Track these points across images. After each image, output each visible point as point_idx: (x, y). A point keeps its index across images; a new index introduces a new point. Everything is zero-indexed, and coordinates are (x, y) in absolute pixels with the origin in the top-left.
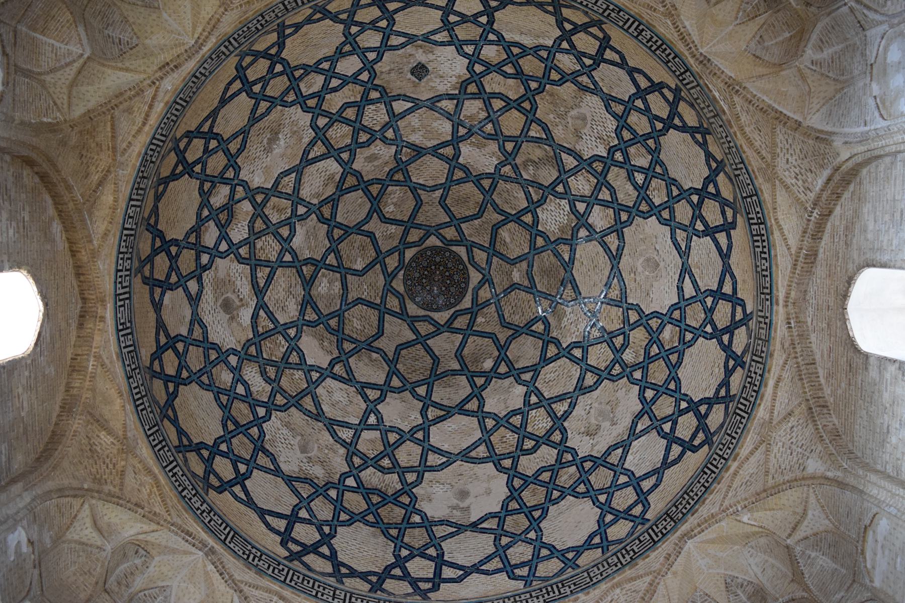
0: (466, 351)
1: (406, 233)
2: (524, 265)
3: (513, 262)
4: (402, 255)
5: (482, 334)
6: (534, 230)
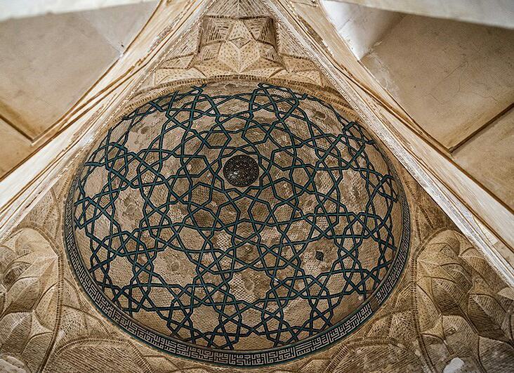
0: (203, 161)
1: (270, 179)
2: (215, 211)
3: (219, 208)
4: (264, 169)
5: (203, 172)
6: (225, 227)
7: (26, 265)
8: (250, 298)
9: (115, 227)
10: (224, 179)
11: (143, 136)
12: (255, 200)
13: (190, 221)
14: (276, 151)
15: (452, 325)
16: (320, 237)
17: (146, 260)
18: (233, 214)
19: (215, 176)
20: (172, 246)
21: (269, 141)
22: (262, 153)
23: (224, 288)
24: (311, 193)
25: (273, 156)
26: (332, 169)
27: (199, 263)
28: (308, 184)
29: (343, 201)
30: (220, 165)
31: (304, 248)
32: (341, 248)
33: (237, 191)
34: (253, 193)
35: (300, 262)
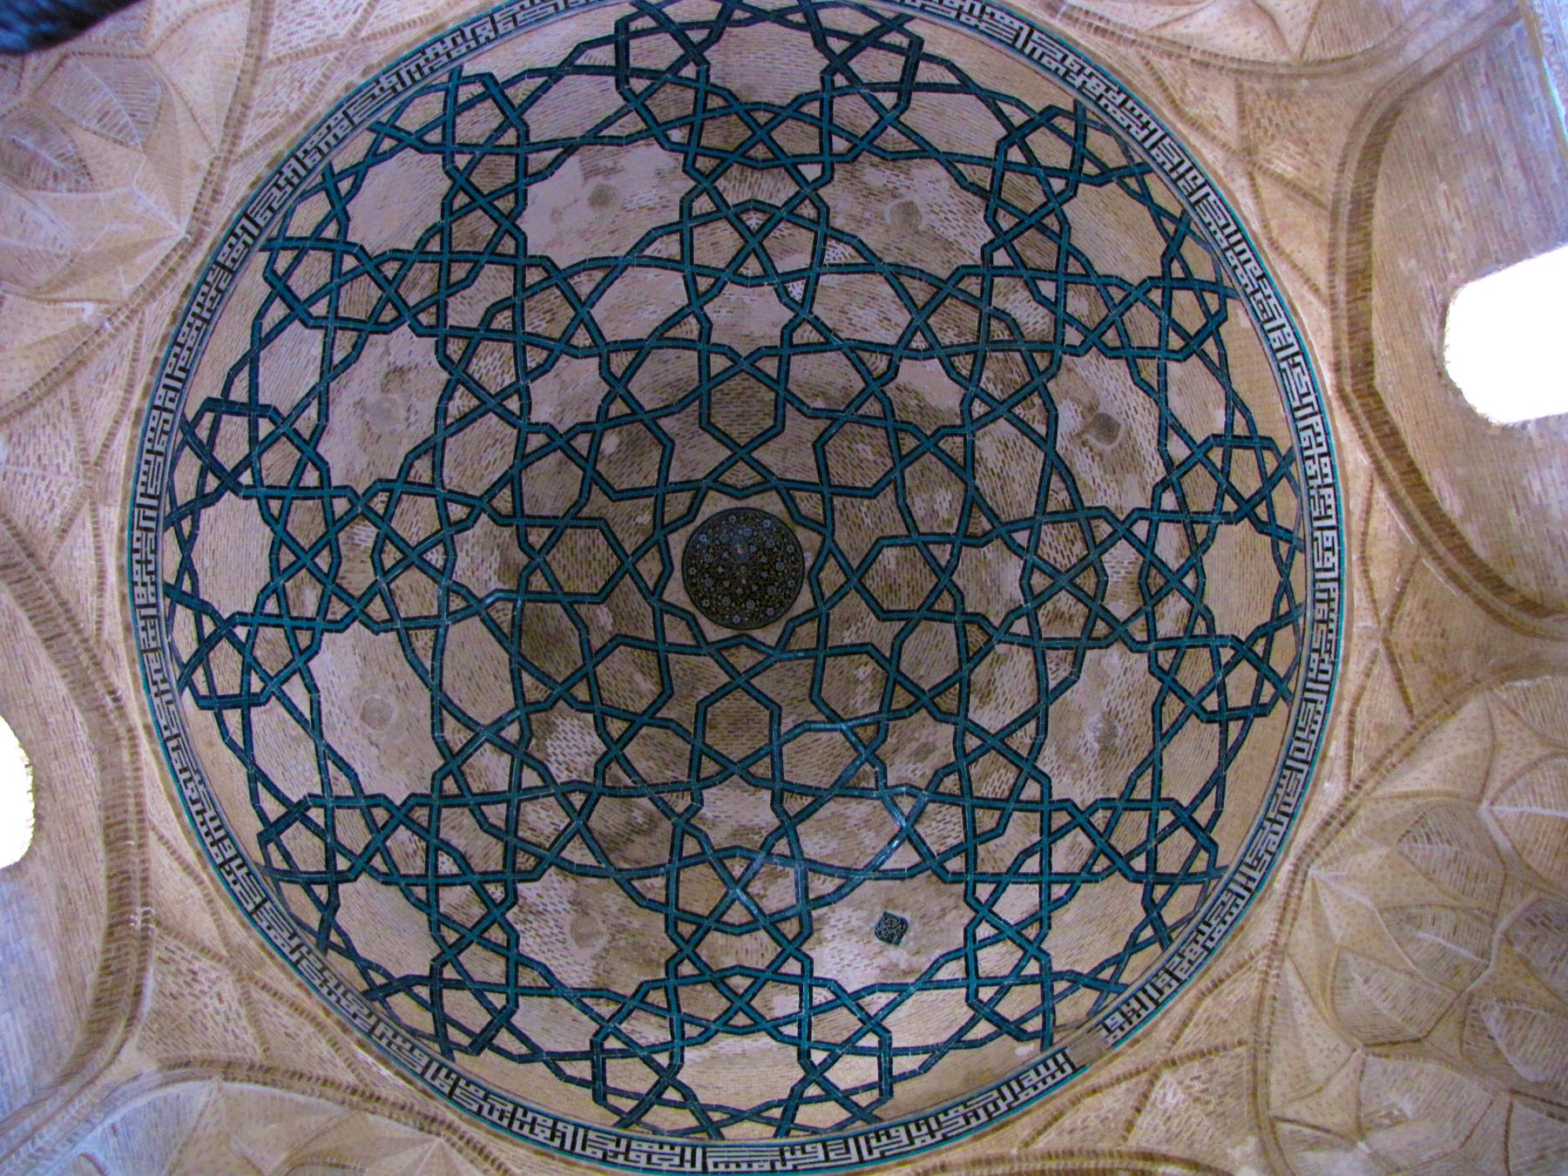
0: (656, 454)
1: (822, 637)
2: (597, 643)
3: (618, 640)
4: (818, 595)
5: (634, 493)
6: (600, 711)
7: (81, 172)
8: (575, 971)
9: (312, 412)
10: (698, 522)
11: (586, 215)
12: (740, 682)
13: (504, 615)
14: (893, 541)
15: (1393, 1097)
16: (913, 872)
17: (310, 610)
18: (648, 687)
19: (656, 539)
20: (406, 644)
21: (888, 498)
22: (842, 538)
23: (496, 892)
24: (940, 716)
25: (870, 558)
26: (1053, 644)
27: (454, 761)
28: (946, 684)
29: (1046, 763)
30: (693, 511)
31: (838, 895)
32: (983, 911)
33: (693, 624)
34: (744, 659)
35: (806, 931)
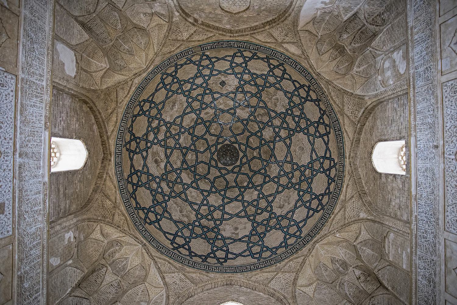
0: (238, 180)
2: (258, 150)
3: (254, 149)
5: (243, 174)
6: (261, 138)
13: (273, 159)
18: (251, 140)
19: (242, 164)
22: (209, 156)
26: (178, 125)
29: (185, 105)
30: (234, 168)
33: (240, 148)
